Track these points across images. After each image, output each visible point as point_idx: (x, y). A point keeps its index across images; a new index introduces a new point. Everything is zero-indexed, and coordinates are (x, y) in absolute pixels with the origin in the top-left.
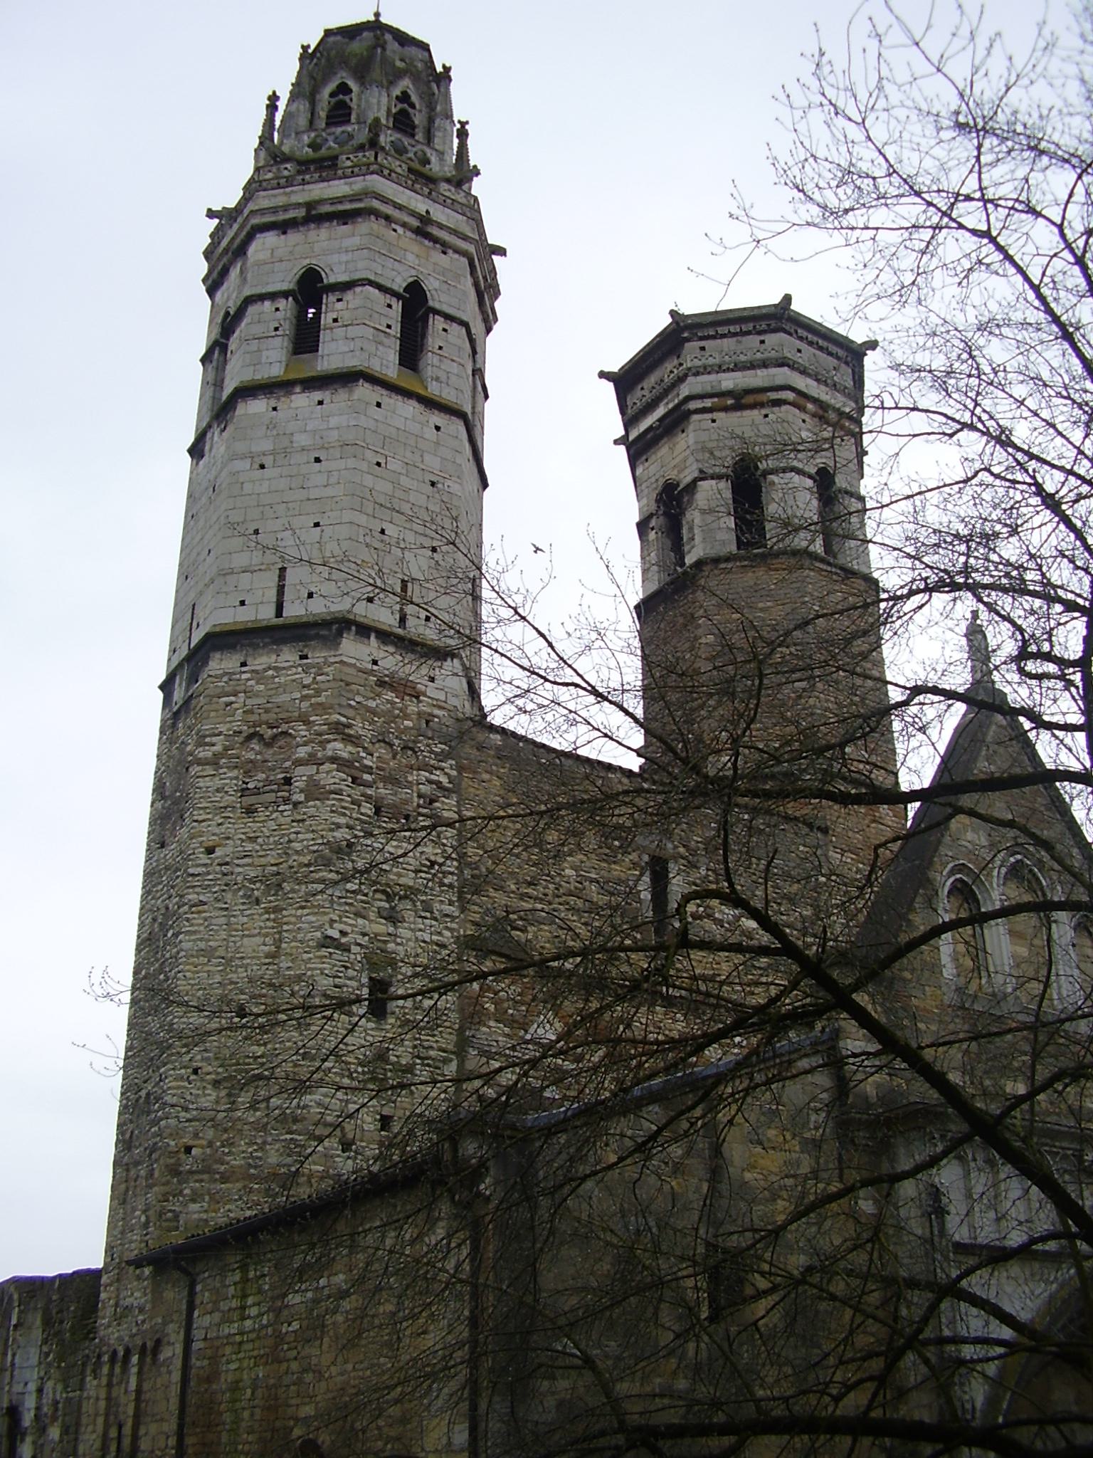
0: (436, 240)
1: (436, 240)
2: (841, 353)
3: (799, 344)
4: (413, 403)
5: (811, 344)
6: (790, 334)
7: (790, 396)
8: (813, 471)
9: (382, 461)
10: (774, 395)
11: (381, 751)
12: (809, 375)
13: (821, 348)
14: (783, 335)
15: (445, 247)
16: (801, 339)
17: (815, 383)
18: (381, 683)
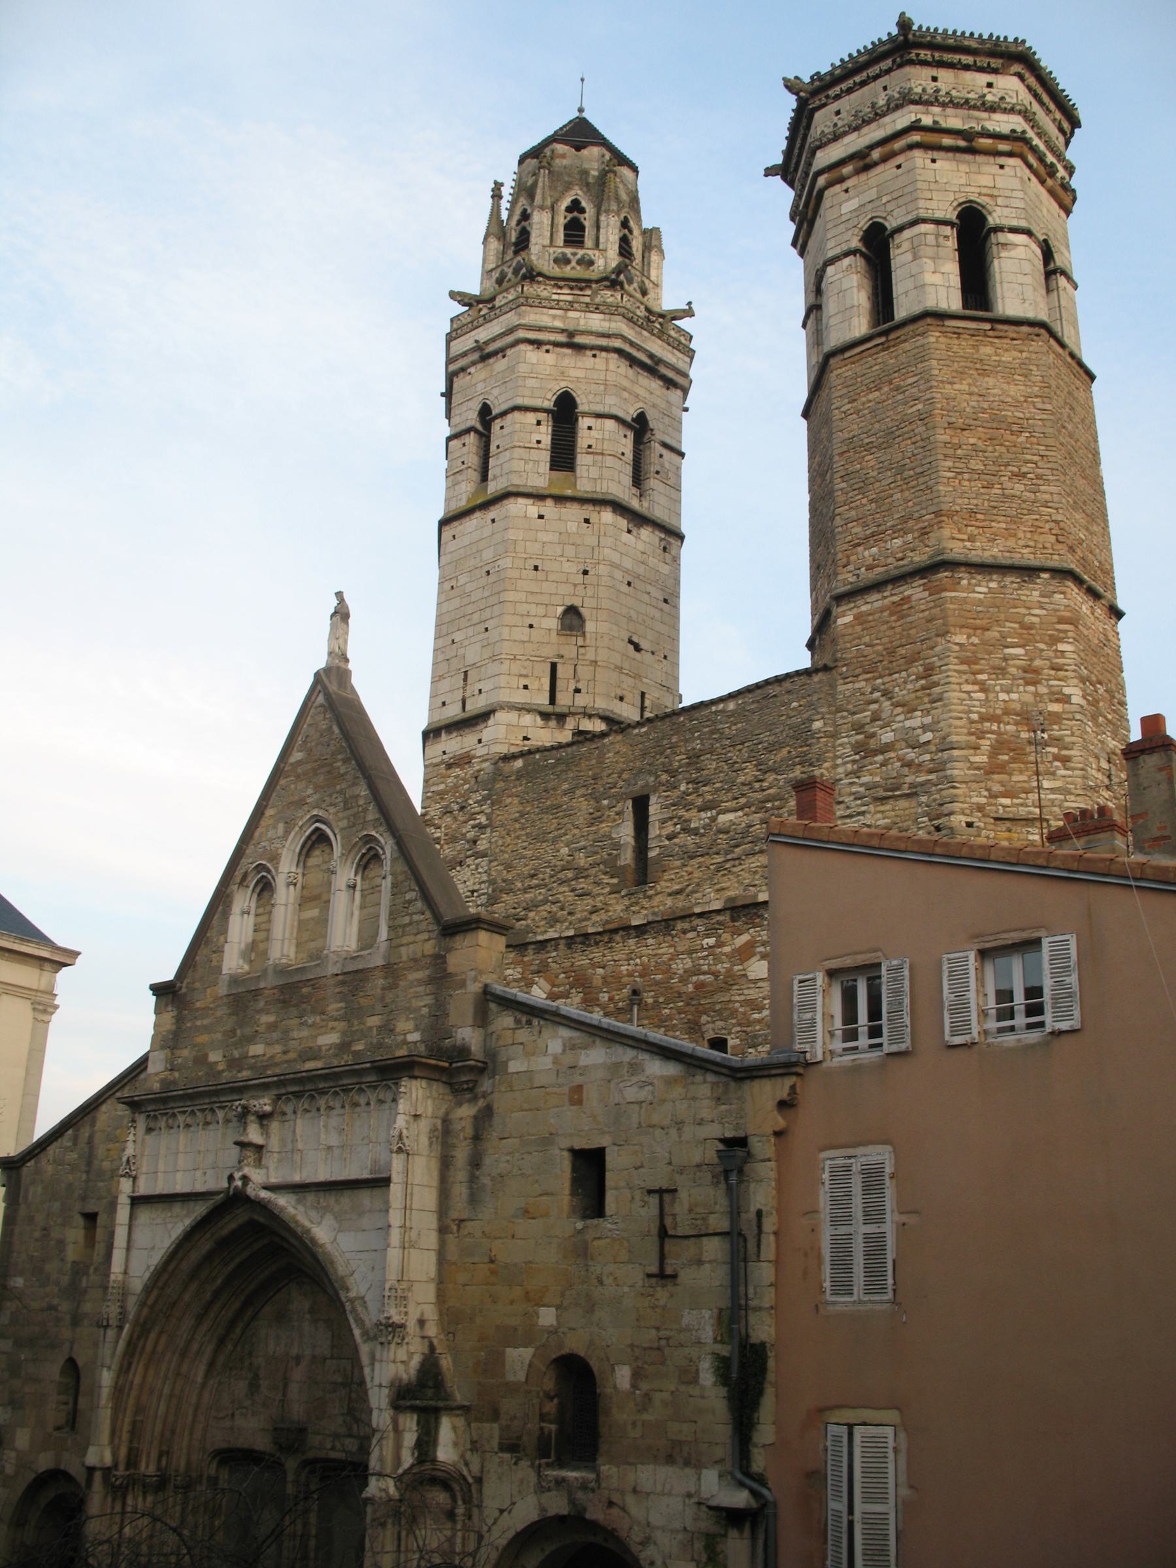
0: (495, 353)
1: (495, 353)
2: (886, 64)
3: (835, 106)
4: (478, 514)
5: (850, 91)
6: (824, 105)
7: (821, 181)
8: (855, 243)
9: (453, 583)
10: (815, 193)
11: (448, 819)
12: (845, 134)
13: (863, 84)
14: (817, 115)
15: (502, 351)
16: (837, 97)
17: (856, 134)
18: (449, 766)
